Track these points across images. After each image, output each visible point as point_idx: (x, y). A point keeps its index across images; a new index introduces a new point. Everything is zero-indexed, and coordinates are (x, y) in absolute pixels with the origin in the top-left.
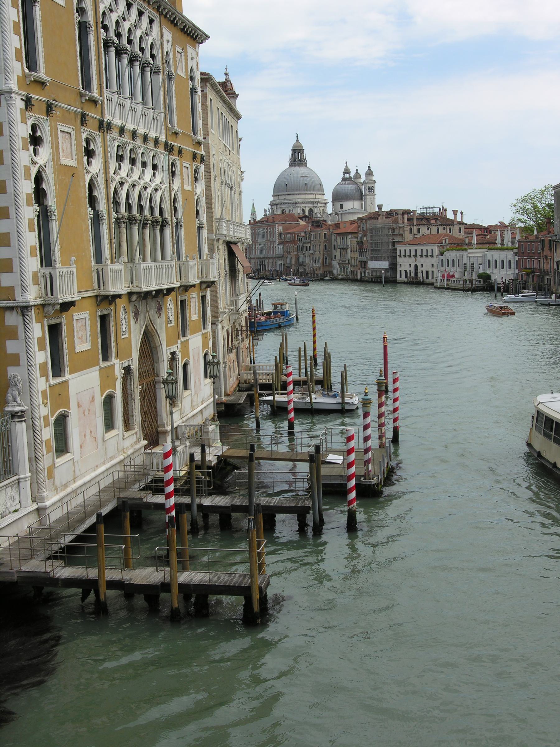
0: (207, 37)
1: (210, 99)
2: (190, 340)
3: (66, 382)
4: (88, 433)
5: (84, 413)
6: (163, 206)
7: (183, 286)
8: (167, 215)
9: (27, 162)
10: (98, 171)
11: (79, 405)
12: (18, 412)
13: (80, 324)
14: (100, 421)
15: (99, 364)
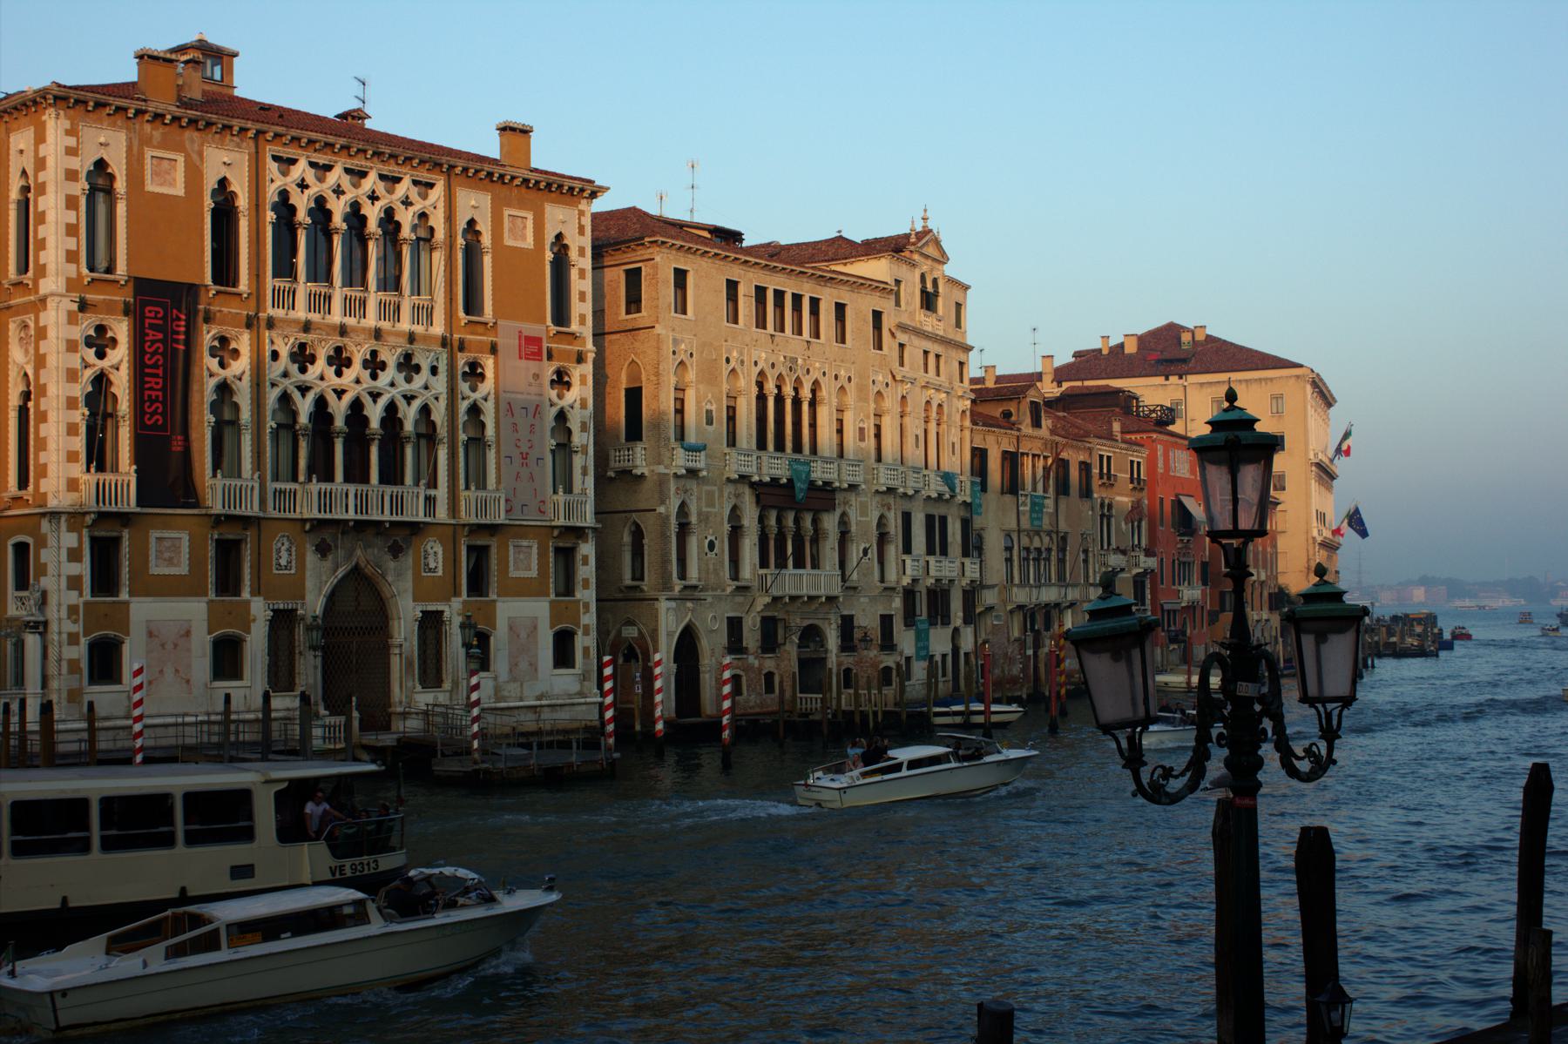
0: (608, 189)
1: (675, 269)
2: (499, 605)
3: (127, 603)
4: (169, 671)
5: (163, 645)
6: (432, 418)
7: (469, 525)
8: (442, 431)
9: (78, 364)
10: (238, 373)
11: (150, 634)
12: (29, 622)
13: (167, 544)
14: (202, 664)
15: (206, 595)
